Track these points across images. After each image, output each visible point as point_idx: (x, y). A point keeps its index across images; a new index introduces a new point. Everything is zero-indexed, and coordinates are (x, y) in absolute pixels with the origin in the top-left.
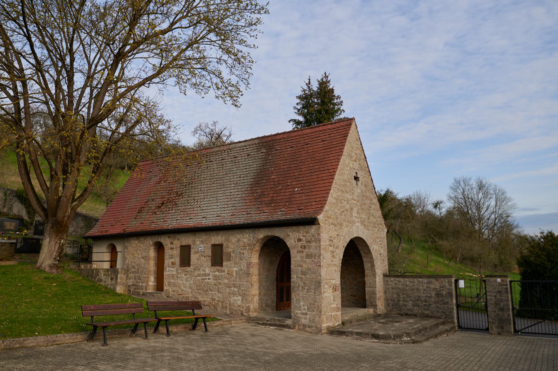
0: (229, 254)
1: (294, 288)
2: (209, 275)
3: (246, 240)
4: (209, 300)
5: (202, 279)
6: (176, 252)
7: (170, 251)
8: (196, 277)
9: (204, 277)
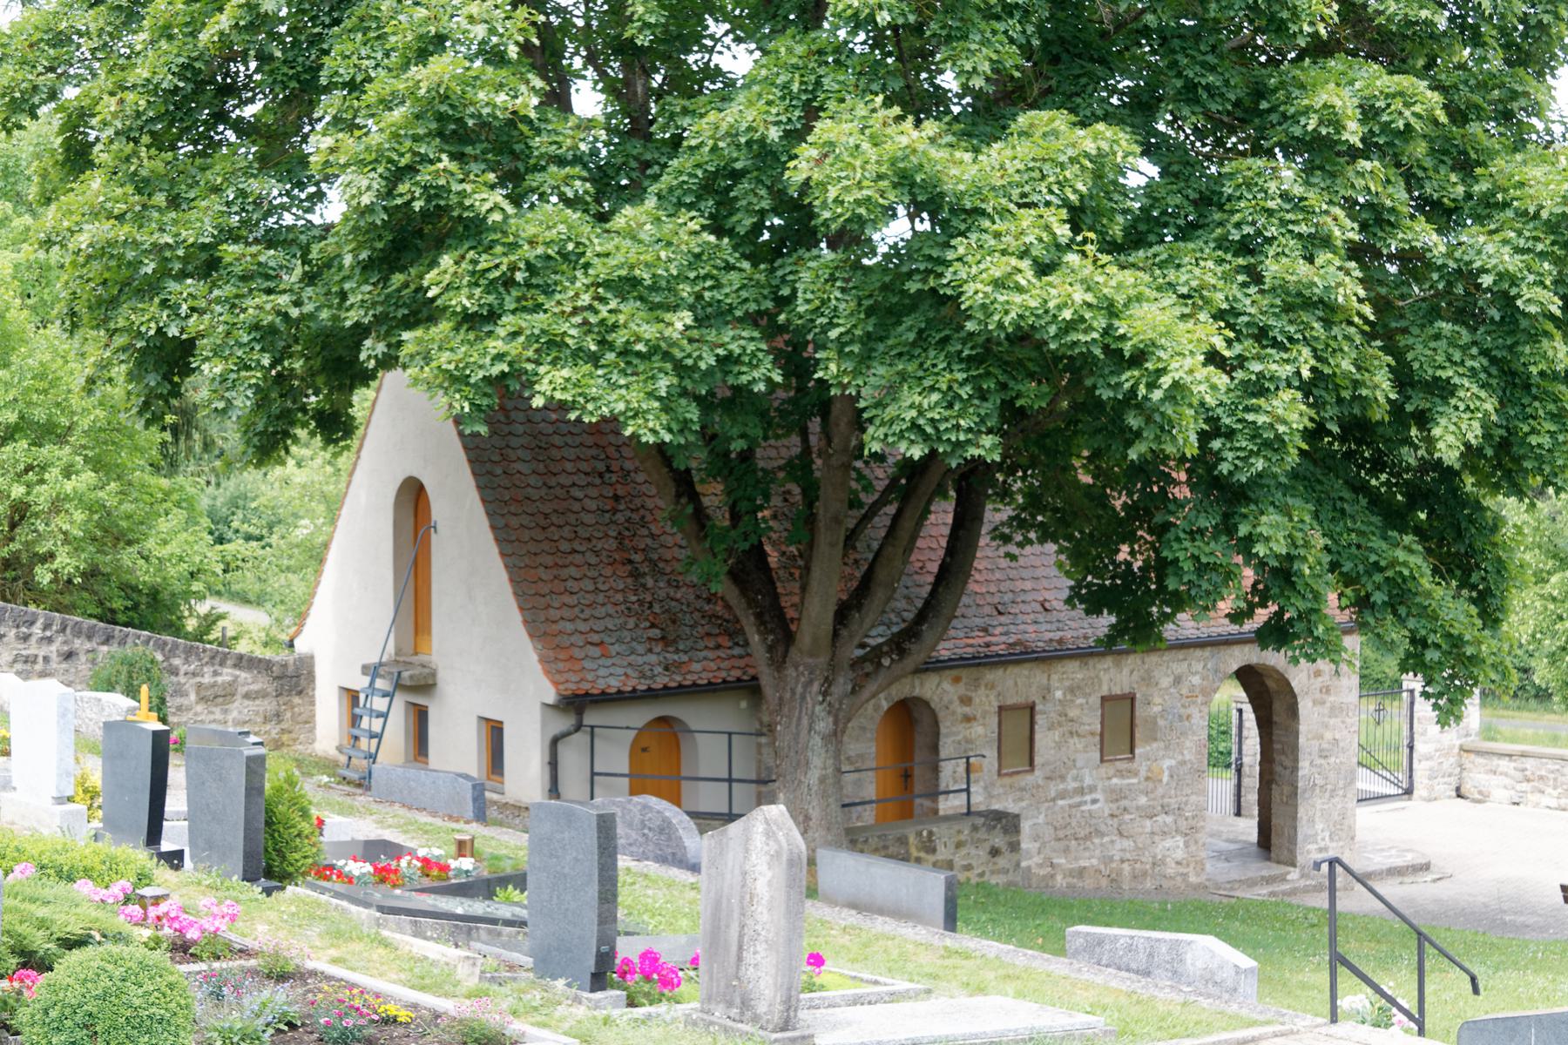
0: (1152, 722)
1: (1305, 791)
2: (1092, 789)
3: (1196, 680)
4: (1094, 862)
5: (1070, 806)
6: (983, 731)
7: (961, 727)
8: (1054, 800)
9: (1077, 799)
